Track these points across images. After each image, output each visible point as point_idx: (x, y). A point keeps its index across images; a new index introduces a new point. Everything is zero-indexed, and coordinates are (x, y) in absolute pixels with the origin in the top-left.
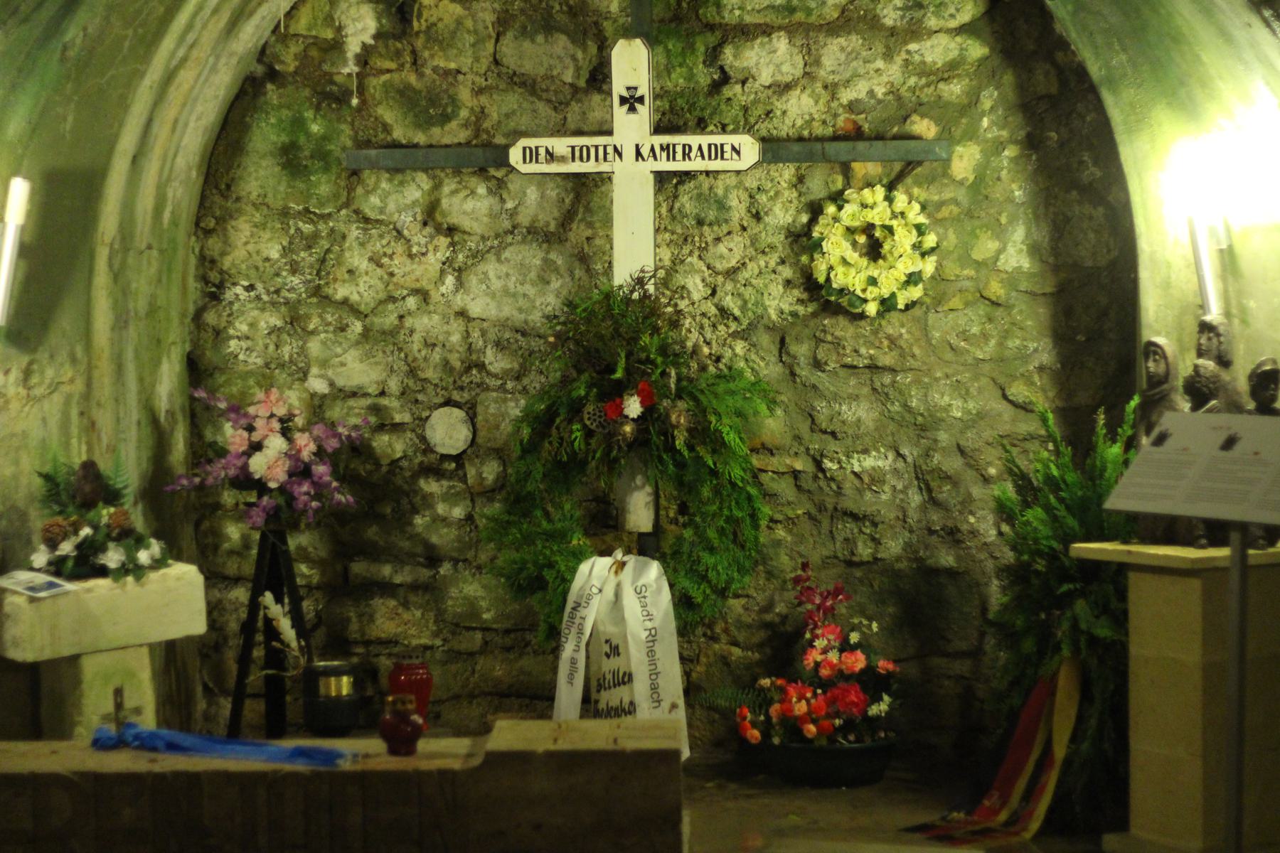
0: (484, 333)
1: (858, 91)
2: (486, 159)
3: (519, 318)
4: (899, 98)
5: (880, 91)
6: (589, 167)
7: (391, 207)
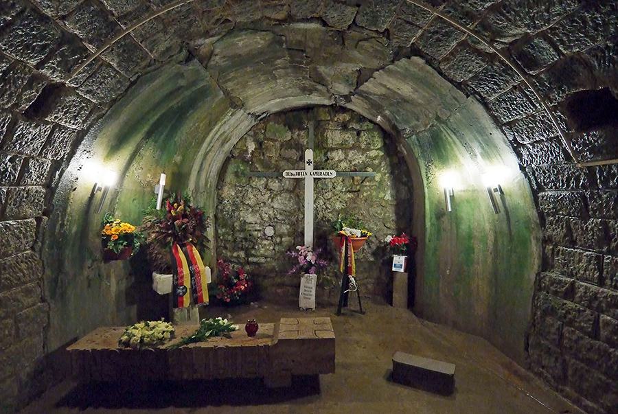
1: (356, 162)
2: (279, 176)
4: (365, 164)
5: (361, 162)
6: (300, 177)
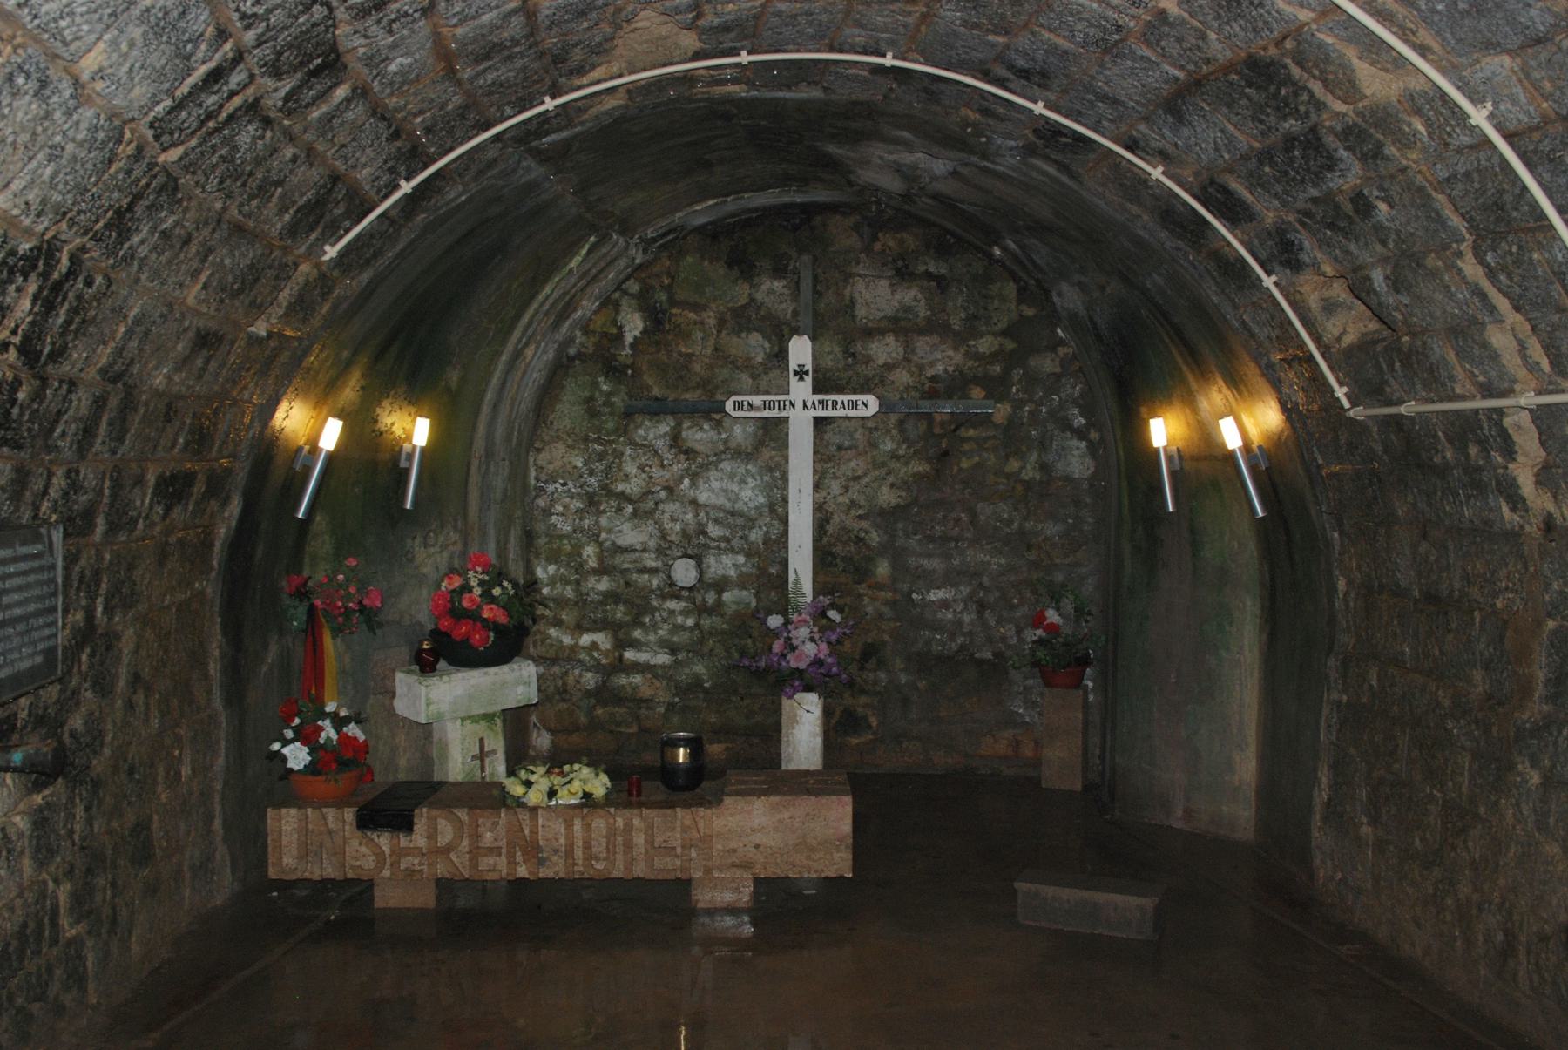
0: (707, 514)
2: (712, 412)
3: (728, 505)
4: (961, 372)
5: (951, 369)
6: (775, 413)
7: (651, 436)
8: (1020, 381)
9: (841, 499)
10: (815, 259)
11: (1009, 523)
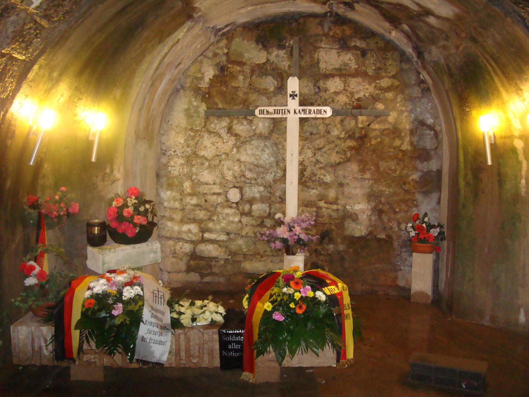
0: (245, 166)
1: (361, 95)
3: (256, 162)
4: (372, 96)
5: (367, 95)
6: (280, 116)
7: (218, 127)
8: (401, 101)
9: (312, 159)
10: (300, 39)
11: (396, 170)
